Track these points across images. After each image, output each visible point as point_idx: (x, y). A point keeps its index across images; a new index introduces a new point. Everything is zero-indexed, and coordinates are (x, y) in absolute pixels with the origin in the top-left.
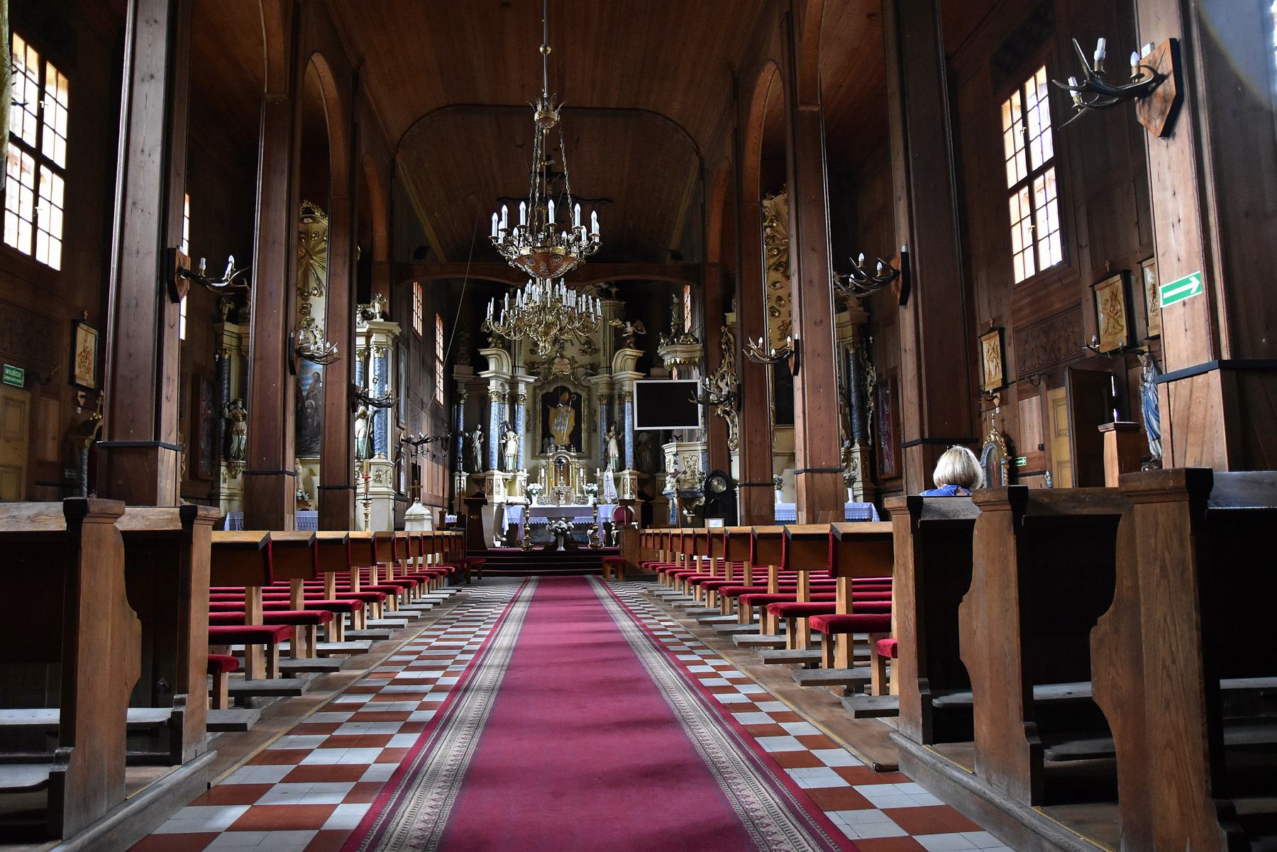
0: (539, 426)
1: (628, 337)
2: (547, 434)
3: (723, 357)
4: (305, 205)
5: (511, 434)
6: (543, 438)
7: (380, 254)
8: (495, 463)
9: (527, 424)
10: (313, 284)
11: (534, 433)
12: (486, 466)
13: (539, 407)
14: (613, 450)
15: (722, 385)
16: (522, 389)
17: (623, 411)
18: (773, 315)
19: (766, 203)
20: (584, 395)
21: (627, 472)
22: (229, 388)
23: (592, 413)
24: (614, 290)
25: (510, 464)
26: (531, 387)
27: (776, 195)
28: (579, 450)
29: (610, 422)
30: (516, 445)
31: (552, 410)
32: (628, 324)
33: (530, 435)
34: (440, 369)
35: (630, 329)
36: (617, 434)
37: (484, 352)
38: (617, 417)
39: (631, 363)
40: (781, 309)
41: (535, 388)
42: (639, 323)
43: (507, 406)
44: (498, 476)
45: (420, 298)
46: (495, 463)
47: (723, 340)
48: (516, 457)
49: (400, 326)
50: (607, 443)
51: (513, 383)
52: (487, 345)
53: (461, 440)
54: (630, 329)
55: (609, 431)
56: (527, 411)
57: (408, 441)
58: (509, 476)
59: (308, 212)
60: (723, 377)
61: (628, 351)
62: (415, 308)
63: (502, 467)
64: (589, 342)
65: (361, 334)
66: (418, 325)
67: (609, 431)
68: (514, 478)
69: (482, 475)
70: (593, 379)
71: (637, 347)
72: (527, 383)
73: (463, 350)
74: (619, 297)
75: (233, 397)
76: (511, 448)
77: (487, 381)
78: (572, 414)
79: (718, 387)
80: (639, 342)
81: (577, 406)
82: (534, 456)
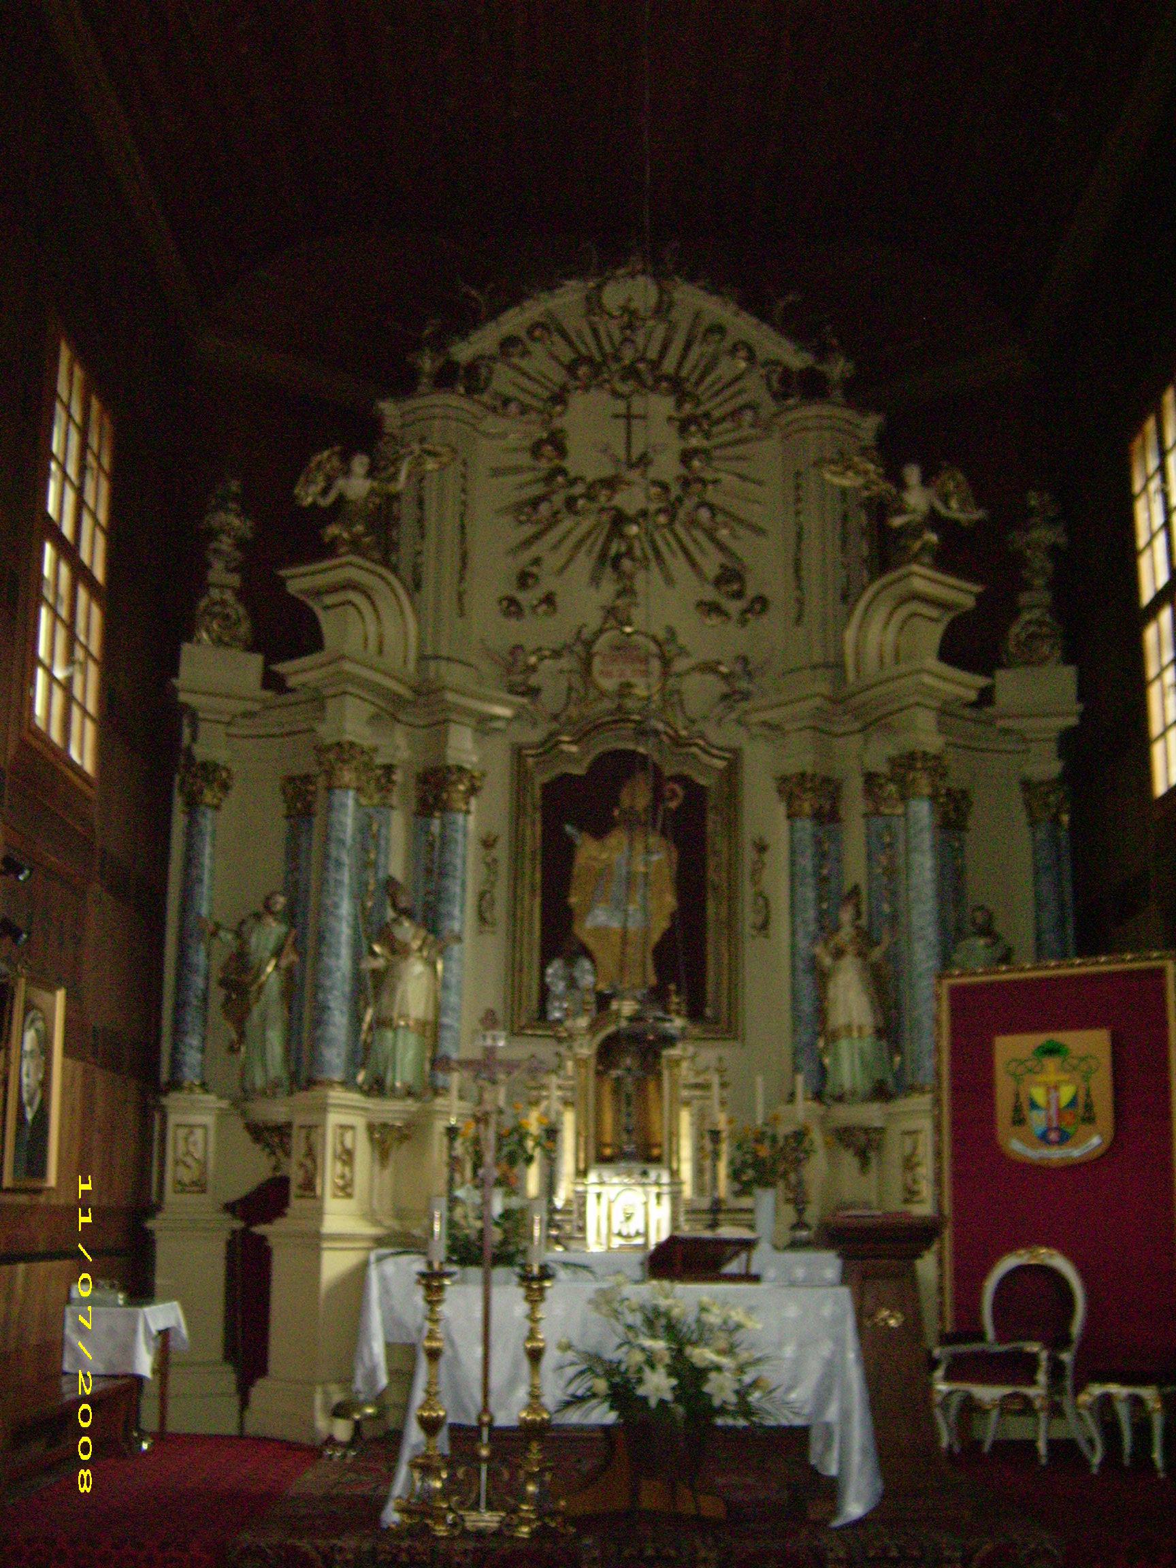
1: (913, 531)
2: (558, 937)
6: (546, 958)
8: (335, 1056)
14: (850, 1000)
24: (838, 368)
25: (405, 1058)
32: (913, 474)
35: (917, 499)
36: (866, 939)
37: (300, 580)
39: (932, 635)
41: (518, 752)
42: (953, 480)
44: (344, 1117)
50: (822, 978)
52: (326, 550)
54: (917, 499)
64: (731, 577)
73: (222, 579)
74: (857, 394)
76: (414, 988)
80: (955, 550)
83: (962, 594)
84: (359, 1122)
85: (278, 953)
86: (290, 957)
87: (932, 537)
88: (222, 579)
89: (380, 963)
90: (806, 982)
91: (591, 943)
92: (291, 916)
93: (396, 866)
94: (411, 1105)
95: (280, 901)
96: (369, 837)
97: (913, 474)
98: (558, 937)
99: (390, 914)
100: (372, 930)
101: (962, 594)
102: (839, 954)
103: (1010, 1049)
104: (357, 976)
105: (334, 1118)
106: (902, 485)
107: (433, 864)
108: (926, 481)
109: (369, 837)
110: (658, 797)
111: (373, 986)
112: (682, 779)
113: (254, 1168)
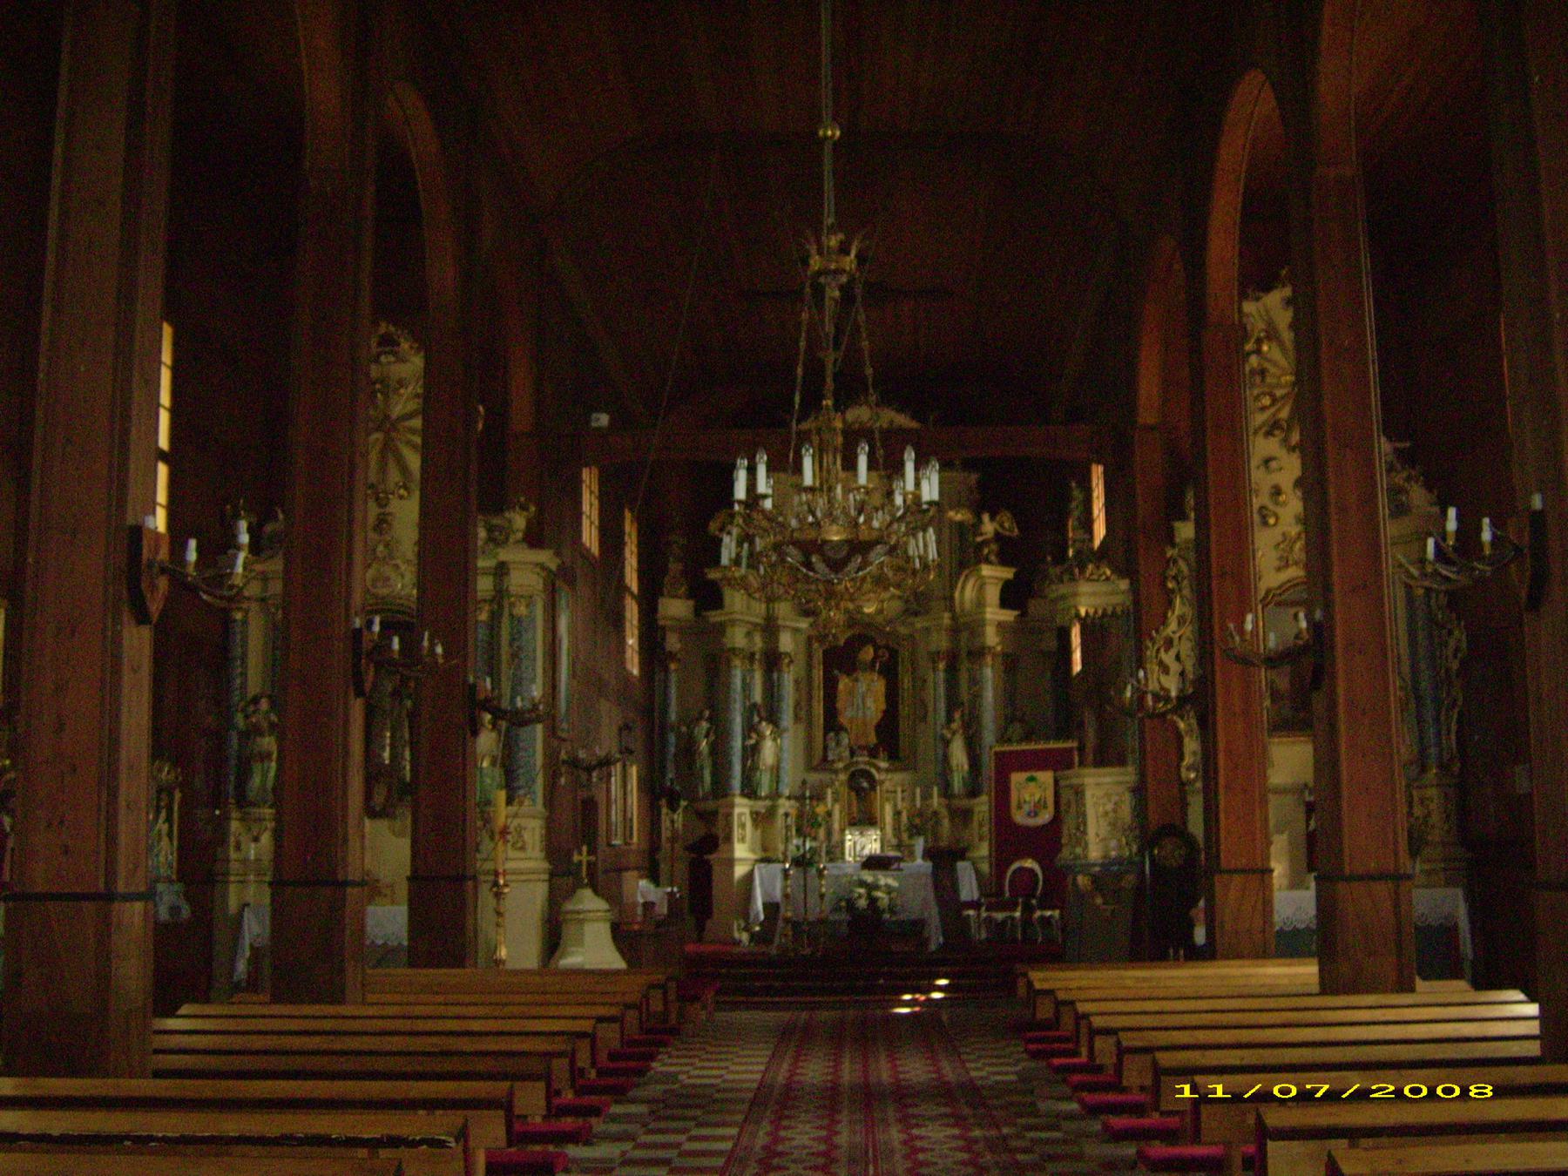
0: (819, 709)
1: (985, 543)
2: (832, 724)
3: (1170, 604)
4: (383, 328)
5: (767, 729)
7: (521, 414)
8: (736, 782)
9: (797, 705)
10: (394, 476)
11: (810, 727)
12: (721, 789)
13: (818, 674)
15: (1168, 658)
16: (786, 642)
17: (975, 681)
18: (1265, 523)
19: (1249, 307)
20: (904, 654)
21: (984, 798)
22: (244, 675)
23: (920, 683)
25: (765, 784)
26: (802, 638)
27: (1268, 289)
28: (893, 756)
29: (953, 703)
30: (779, 750)
31: (844, 683)
32: (986, 517)
33: (801, 727)
34: (632, 612)
36: (966, 726)
38: (965, 696)
39: (993, 594)
40: (1280, 511)
41: (809, 640)
43: (758, 677)
44: (742, 809)
45: (595, 488)
46: (736, 782)
47: (1173, 572)
48: (776, 770)
49: (558, 554)
50: (947, 743)
51: (770, 628)
53: (672, 738)
55: (950, 719)
56: (796, 682)
57: (574, 763)
58: (761, 806)
59: (388, 342)
60: (1169, 643)
61: (986, 570)
62: (586, 508)
63: (750, 791)
65: (485, 572)
66: (590, 536)
67: (950, 719)
68: (771, 812)
69: (710, 805)
70: (920, 623)
71: (1004, 561)
72: (796, 630)
73: (675, 567)
75: (254, 687)
76: (768, 751)
77: (720, 629)
78: (880, 686)
79: (1161, 663)
80: (1007, 552)
81: (890, 672)
82: (810, 767)
83: (1008, 573)
84: (747, 811)
85: (707, 736)
86: (712, 738)
87: (994, 547)
88: (675, 567)
89: (752, 742)
90: (940, 745)
91: (848, 726)
92: (710, 719)
93: (758, 696)
94: (768, 803)
95: (707, 713)
96: (747, 687)
97: (986, 517)
98: (832, 724)
99: (756, 719)
100: (750, 728)
101: (1008, 573)
102: (954, 733)
103: (1017, 778)
104: (744, 748)
105: (737, 811)
106: (980, 521)
107: (771, 690)
108: (992, 519)
109: (747, 687)
110: (876, 657)
111: (751, 752)
112: (887, 647)
113: (700, 830)
